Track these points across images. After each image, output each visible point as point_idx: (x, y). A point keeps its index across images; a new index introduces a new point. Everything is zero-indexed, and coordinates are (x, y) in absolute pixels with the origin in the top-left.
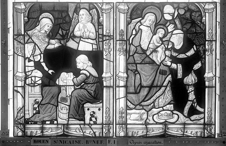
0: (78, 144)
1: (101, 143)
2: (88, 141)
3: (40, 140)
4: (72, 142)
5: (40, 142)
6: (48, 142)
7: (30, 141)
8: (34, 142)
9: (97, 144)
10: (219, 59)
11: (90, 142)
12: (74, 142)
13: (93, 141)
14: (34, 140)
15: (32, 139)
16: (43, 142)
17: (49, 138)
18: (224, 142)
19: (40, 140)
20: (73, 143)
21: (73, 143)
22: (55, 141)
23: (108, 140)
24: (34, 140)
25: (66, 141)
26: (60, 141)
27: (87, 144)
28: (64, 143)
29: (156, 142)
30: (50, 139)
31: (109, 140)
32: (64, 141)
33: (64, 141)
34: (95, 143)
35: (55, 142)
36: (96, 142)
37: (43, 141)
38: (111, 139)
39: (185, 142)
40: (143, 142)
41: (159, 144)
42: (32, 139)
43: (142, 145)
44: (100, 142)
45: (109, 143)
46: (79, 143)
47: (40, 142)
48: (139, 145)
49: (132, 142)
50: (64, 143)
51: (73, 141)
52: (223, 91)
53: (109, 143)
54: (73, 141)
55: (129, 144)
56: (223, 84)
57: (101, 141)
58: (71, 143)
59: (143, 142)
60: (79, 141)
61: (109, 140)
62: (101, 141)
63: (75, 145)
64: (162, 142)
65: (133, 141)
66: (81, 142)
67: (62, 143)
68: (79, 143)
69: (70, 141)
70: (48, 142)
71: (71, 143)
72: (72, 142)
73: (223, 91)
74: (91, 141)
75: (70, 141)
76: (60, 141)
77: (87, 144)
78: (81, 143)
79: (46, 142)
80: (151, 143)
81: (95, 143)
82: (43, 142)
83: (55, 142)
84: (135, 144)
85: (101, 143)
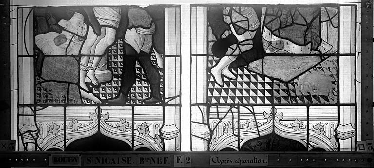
0: (126, 164)
1: (165, 163)
2: (143, 159)
3: (64, 158)
4: (116, 161)
5: (64, 161)
6: (77, 161)
8: (55, 161)
9: (158, 163)
10: (360, 22)
11: (147, 161)
12: (121, 160)
13: (152, 158)
15: (50, 155)
17: (79, 155)
18: (369, 160)
20: (118, 163)
21: (118, 163)
22: (89, 159)
25: (106, 160)
26: (97, 158)
28: (103, 163)
31: (178, 157)
32: (103, 158)
33: (103, 158)
34: (154, 162)
37: (69, 158)
38: (180, 155)
39: (304, 159)
42: (50, 155)
43: (231, 164)
44: (163, 160)
45: (178, 162)
46: (128, 163)
47: (64, 161)
48: (227, 164)
49: (215, 160)
50: (103, 163)
52: (367, 76)
53: (178, 162)
55: (212, 163)
56: (367, 64)
57: (165, 158)
58: (115, 163)
60: (128, 158)
61: (178, 157)
62: (165, 158)
63: (122, 165)
64: (265, 161)
65: (218, 158)
68: (128, 163)
70: (77, 161)
72: (116, 161)
73: (367, 76)
74: (148, 159)
76: (97, 158)
77: (141, 163)
78: (132, 163)
80: (247, 161)
81: (154, 162)
82: (69, 161)
83: (88, 159)
84: (221, 163)
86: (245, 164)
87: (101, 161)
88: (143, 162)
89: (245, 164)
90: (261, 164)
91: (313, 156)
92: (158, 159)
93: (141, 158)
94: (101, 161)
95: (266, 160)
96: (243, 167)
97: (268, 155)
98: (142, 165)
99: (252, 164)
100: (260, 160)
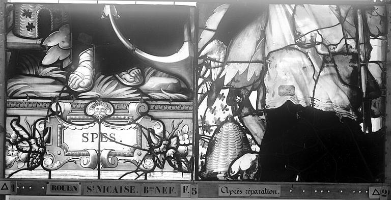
0: (129, 194)
1: (170, 193)
2: (147, 188)
3: (63, 186)
4: (119, 190)
5: (63, 190)
6: (76, 190)
7: (45, 187)
8: (53, 189)
9: (163, 193)
11: (152, 190)
12: (123, 189)
14: (53, 186)
15: (48, 183)
16: (68, 190)
17: (78, 183)
19: (63, 186)
20: (121, 192)
21: (121, 192)
23: (182, 186)
24: (53, 186)
27: (145, 193)
28: (104, 192)
29: (267, 190)
30: (80, 184)
31: (184, 187)
32: (104, 187)
33: (104, 187)
34: (159, 192)
35: (91, 190)
36: (161, 190)
37: (68, 186)
38: (187, 185)
40: (244, 192)
41: (272, 195)
42: (48, 183)
43: (241, 195)
45: (184, 192)
46: (131, 192)
47: (63, 190)
50: (104, 192)
51: (121, 187)
53: (184, 192)
54: (121, 187)
55: (220, 194)
57: (170, 188)
58: (117, 192)
59: (244, 192)
60: (131, 187)
61: (184, 187)
62: (170, 188)
63: (125, 194)
64: (278, 191)
66: (135, 190)
67: (100, 190)
68: (131, 192)
69: (115, 188)
70: (76, 190)
71: (117, 192)
72: (119, 190)
74: (153, 188)
75: (115, 188)
76: (98, 187)
77: (145, 193)
79: (74, 189)
82: (68, 190)
83: (91, 190)
84: (231, 193)
85: (170, 193)
86: (256, 195)
87: (102, 190)
88: (148, 192)
89: (256, 195)
90: (272, 195)
91: (329, 187)
92: (164, 188)
93: (145, 187)
94: (102, 190)
95: (278, 191)
96: (252, 198)
97: (280, 186)
98: (146, 194)
99: (263, 195)
100: (272, 191)
